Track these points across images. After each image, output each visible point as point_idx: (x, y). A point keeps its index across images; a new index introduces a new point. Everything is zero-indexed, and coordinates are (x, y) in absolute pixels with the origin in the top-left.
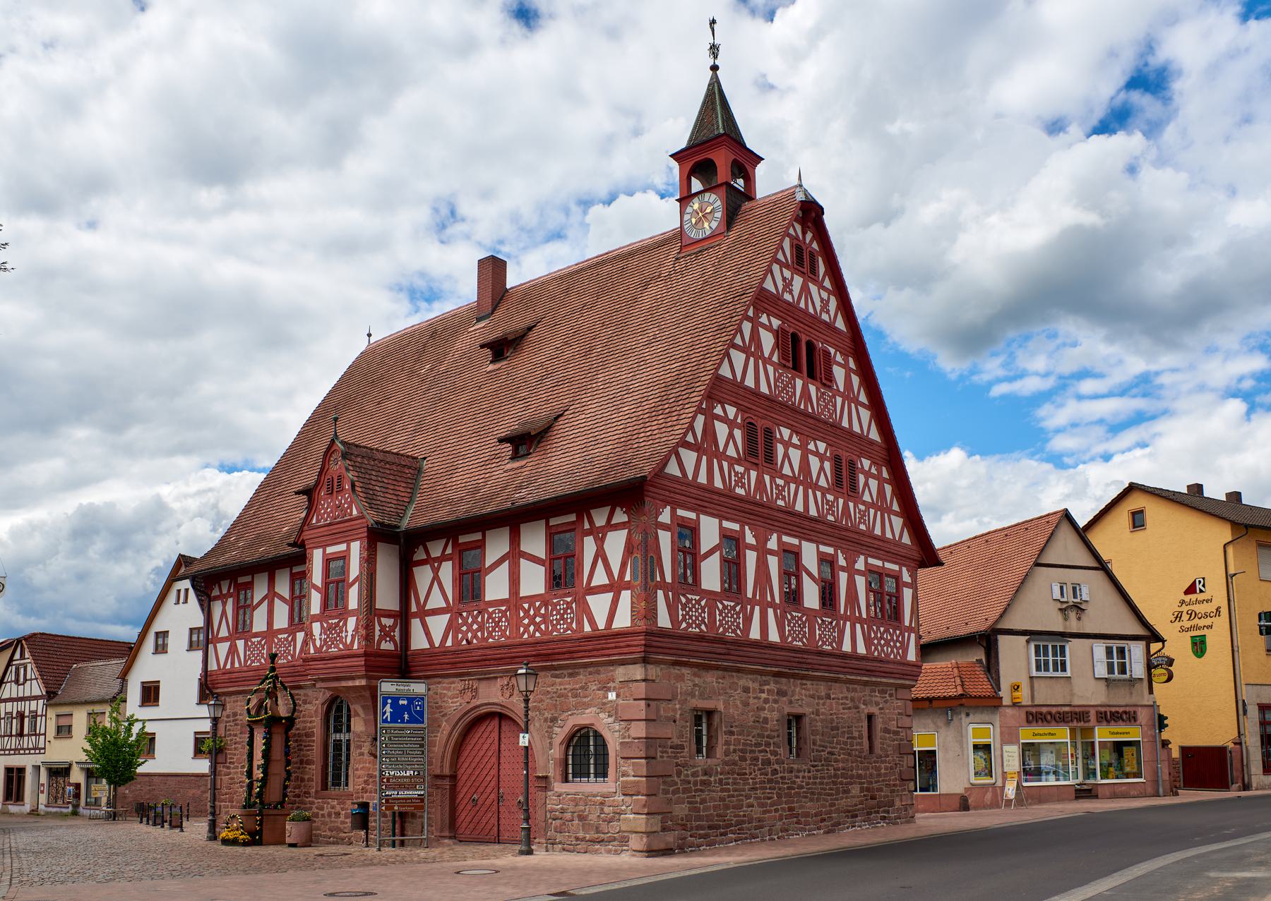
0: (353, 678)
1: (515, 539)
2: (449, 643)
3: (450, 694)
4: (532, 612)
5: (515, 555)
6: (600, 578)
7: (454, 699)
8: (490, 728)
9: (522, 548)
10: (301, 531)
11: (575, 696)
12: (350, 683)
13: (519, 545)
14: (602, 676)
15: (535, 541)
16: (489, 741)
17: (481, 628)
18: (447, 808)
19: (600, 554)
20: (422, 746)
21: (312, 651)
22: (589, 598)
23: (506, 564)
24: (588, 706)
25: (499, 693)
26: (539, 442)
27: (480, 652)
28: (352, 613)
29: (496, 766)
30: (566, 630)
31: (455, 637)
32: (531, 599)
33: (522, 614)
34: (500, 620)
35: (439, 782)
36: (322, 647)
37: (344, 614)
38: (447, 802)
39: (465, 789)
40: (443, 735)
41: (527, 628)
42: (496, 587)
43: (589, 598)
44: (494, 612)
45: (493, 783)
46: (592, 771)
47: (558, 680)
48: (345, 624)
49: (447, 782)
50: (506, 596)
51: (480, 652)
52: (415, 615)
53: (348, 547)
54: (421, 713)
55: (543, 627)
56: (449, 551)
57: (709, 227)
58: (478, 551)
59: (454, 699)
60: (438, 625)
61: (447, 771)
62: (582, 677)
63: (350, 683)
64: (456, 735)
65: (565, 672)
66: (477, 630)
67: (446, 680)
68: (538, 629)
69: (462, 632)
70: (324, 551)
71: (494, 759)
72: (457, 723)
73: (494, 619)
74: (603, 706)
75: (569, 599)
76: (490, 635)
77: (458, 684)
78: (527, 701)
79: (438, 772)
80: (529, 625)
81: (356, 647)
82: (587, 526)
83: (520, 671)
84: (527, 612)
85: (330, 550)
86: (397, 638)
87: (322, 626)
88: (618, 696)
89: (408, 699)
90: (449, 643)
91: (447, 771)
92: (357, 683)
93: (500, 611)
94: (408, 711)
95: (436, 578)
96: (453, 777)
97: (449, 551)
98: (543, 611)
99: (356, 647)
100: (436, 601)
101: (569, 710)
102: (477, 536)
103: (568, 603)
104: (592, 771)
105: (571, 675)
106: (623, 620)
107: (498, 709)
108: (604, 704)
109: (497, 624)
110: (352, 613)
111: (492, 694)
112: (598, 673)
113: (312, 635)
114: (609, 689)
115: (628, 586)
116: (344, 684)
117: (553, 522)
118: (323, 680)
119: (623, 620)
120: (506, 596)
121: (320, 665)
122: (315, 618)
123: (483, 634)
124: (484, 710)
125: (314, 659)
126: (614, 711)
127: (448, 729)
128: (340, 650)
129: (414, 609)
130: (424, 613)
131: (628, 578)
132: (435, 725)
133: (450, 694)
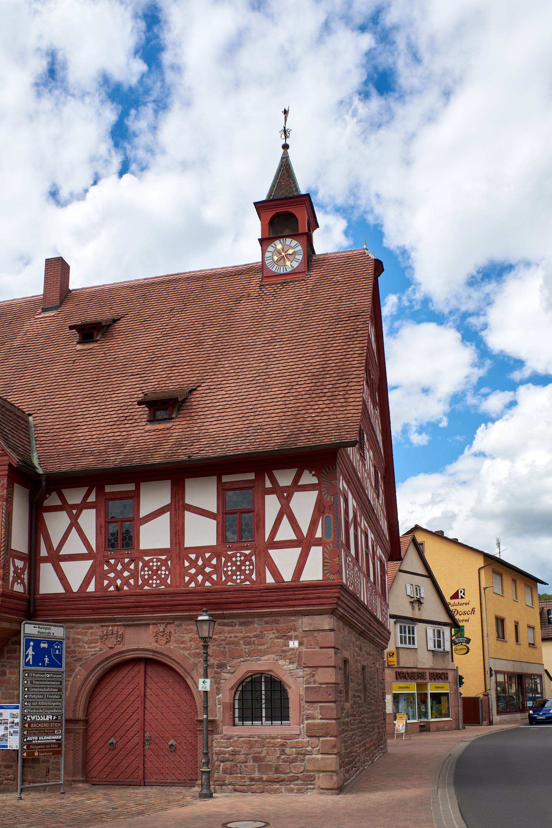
1: (178, 493)
2: (91, 588)
3: (86, 639)
4: (200, 562)
5: (177, 509)
6: (286, 532)
7: (93, 644)
8: (132, 674)
9: (187, 502)
11: (249, 644)
13: (183, 498)
14: (282, 626)
15: (203, 495)
16: (131, 686)
17: (134, 575)
18: (80, 752)
19: (286, 511)
20: (60, 690)
22: (271, 552)
23: (167, 516)
24: (265, 653)
25: (153, 640)
26: (179, 410)
27: (133, 599)
29: (141, 710)
30: (243, 581)
31: (99, 584)
32: (200, 551)
33: (187, 564)
34: (159, 568)
35: (71, 726)
38: (80, 746)
39: (98, 734)
40: (78, 678)
41: (193, 578)
42: (154, 536)
43: (271, 552)
44: (151, 561)
45: (136, 728)
46: (264, 715)
47: (226, 629)
49: (80, 727)
50: (168, 546)
51: (133, 599)
52: (45, 560)
54: (59, 657)
55: (214, 577)
56: (92, 498)
57: (290, 265)
58: (131, 501)
59: (93, 644)
60: (77, 573)
61: (80, 715)
62: (257, 626)
64: (93, 679)
65: (235, 621)
66: (129, 577)
67: (82, 626)
68: (207, 577)
69: (109, 579)
71: (137, 704)
72: (95, 668)
73: (150, 568)
74: (284, 653)
75: (247, 552)
76: (146, 582)
77: (97, 630)
78: (206, 647)
79: (70, 716)
80: (196, 575)
82: (268, 484)
83: (200, 618)
84: (193, 563)
86: (26, 581)
88: (301, 644)
89: (48, 642)
90: (91, 588)
91: (80, 715)
93: (158, 560)
94: (48, 654)
95: (74, 524)
96: (86, 721)
97: (92, 498)
98: (214, 562)
100: (74, 545)
101: (241, 656)
102: (131, 487)
103: (245, 555)
104: (264, 715)
105: (242, 624)
106: (313, 572)
107: (149, 655)
108: (285, 651)
109: (155, 572)
111: (142, 640)
112: (277, 622)
114: (290, 638)
115: (318, 542)
117: (226, 479)
119: (313, 572)
120: (168, 546)
123: (136, 581)
124: (128, 656)
126: (296, 658)
127: (84, 673)
129: (44, 552)
130: (56, 559)
131: (319, 534)
132: (70, 670)
133: (86, 639)
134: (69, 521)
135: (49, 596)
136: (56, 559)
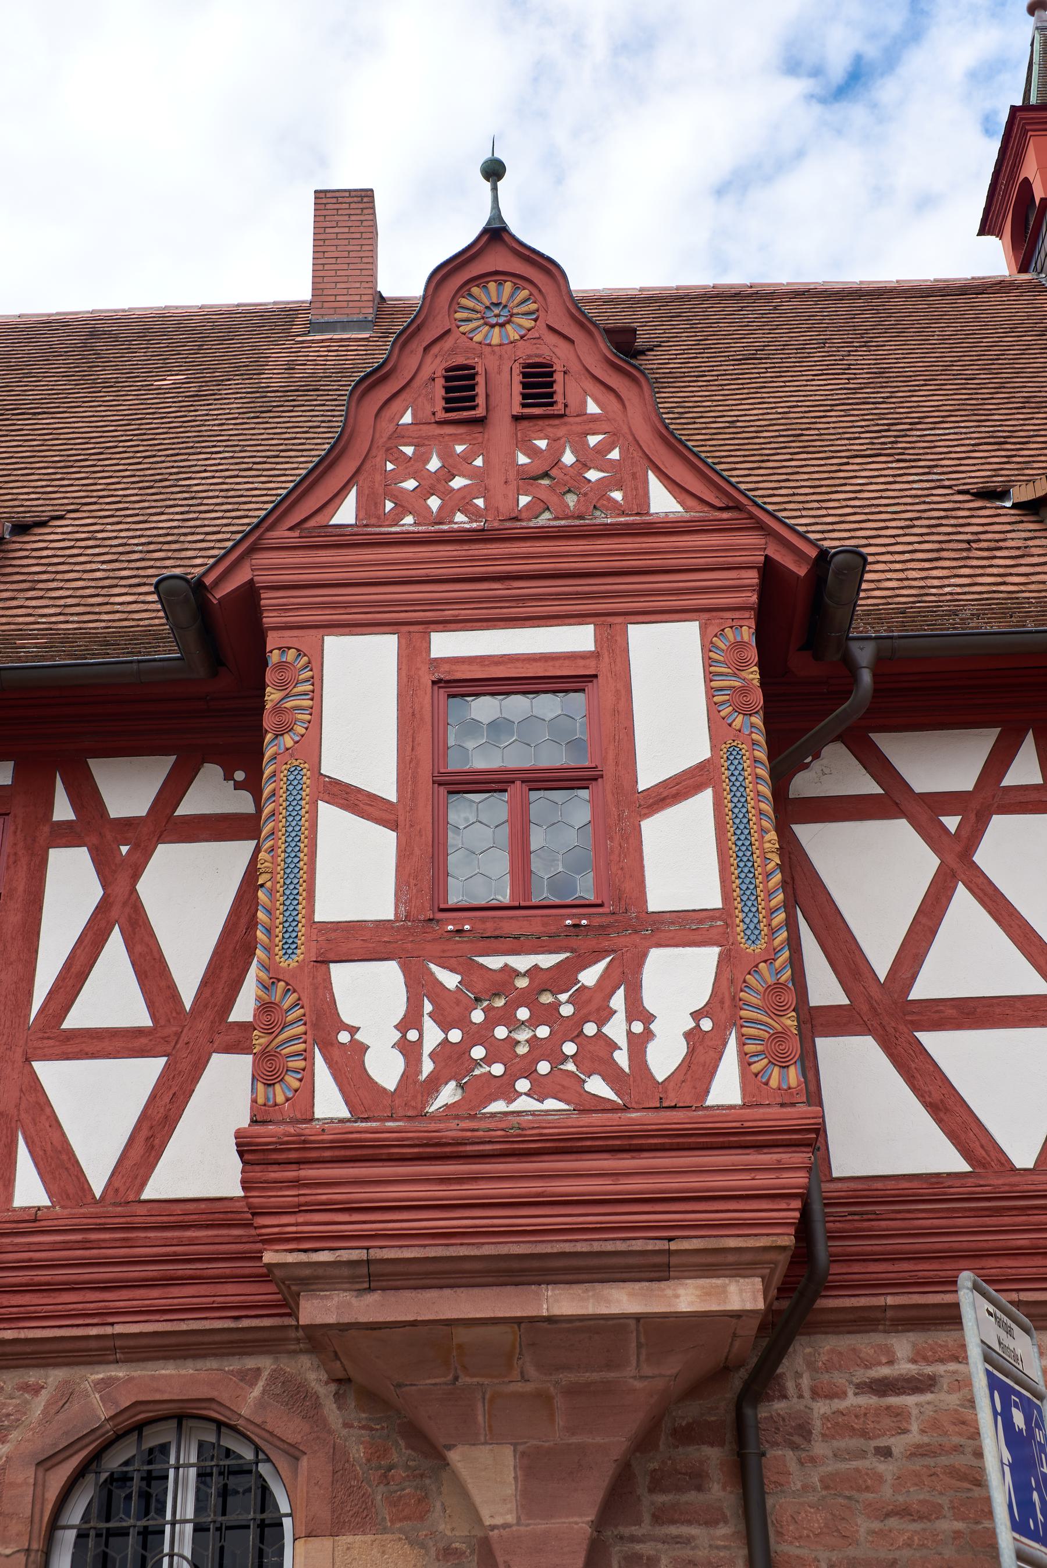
0: (659, 1269)
10: (252, 542)
12: (623, 1300)
21: (329, 1103)
28: (684, 928)
36: (415, 1088)
37: (616, 925)
48: (628, 975)
53: (613, 650)
63: (623, 1300)
70: (412, 657)
81: (726, 1089)
85: (445, 645)
87: (419, 985)
92: (686, 1297)
99: (726, 1089)
110: (684, 928)
113: (324, 1022)
116: (563, 1302)
118: (373, 1277)
121: (403, 1184)
122: (360, 942)
125: (347, 1149)
128: (600, 1105)
134: (926, 863)
135: (890, 1184)
136: (894, 1016)
